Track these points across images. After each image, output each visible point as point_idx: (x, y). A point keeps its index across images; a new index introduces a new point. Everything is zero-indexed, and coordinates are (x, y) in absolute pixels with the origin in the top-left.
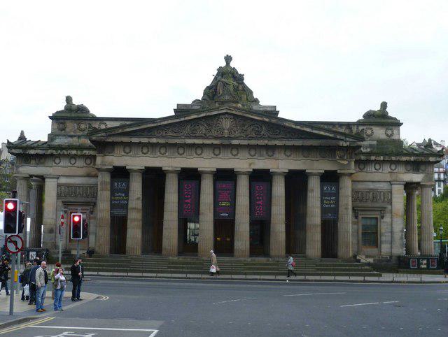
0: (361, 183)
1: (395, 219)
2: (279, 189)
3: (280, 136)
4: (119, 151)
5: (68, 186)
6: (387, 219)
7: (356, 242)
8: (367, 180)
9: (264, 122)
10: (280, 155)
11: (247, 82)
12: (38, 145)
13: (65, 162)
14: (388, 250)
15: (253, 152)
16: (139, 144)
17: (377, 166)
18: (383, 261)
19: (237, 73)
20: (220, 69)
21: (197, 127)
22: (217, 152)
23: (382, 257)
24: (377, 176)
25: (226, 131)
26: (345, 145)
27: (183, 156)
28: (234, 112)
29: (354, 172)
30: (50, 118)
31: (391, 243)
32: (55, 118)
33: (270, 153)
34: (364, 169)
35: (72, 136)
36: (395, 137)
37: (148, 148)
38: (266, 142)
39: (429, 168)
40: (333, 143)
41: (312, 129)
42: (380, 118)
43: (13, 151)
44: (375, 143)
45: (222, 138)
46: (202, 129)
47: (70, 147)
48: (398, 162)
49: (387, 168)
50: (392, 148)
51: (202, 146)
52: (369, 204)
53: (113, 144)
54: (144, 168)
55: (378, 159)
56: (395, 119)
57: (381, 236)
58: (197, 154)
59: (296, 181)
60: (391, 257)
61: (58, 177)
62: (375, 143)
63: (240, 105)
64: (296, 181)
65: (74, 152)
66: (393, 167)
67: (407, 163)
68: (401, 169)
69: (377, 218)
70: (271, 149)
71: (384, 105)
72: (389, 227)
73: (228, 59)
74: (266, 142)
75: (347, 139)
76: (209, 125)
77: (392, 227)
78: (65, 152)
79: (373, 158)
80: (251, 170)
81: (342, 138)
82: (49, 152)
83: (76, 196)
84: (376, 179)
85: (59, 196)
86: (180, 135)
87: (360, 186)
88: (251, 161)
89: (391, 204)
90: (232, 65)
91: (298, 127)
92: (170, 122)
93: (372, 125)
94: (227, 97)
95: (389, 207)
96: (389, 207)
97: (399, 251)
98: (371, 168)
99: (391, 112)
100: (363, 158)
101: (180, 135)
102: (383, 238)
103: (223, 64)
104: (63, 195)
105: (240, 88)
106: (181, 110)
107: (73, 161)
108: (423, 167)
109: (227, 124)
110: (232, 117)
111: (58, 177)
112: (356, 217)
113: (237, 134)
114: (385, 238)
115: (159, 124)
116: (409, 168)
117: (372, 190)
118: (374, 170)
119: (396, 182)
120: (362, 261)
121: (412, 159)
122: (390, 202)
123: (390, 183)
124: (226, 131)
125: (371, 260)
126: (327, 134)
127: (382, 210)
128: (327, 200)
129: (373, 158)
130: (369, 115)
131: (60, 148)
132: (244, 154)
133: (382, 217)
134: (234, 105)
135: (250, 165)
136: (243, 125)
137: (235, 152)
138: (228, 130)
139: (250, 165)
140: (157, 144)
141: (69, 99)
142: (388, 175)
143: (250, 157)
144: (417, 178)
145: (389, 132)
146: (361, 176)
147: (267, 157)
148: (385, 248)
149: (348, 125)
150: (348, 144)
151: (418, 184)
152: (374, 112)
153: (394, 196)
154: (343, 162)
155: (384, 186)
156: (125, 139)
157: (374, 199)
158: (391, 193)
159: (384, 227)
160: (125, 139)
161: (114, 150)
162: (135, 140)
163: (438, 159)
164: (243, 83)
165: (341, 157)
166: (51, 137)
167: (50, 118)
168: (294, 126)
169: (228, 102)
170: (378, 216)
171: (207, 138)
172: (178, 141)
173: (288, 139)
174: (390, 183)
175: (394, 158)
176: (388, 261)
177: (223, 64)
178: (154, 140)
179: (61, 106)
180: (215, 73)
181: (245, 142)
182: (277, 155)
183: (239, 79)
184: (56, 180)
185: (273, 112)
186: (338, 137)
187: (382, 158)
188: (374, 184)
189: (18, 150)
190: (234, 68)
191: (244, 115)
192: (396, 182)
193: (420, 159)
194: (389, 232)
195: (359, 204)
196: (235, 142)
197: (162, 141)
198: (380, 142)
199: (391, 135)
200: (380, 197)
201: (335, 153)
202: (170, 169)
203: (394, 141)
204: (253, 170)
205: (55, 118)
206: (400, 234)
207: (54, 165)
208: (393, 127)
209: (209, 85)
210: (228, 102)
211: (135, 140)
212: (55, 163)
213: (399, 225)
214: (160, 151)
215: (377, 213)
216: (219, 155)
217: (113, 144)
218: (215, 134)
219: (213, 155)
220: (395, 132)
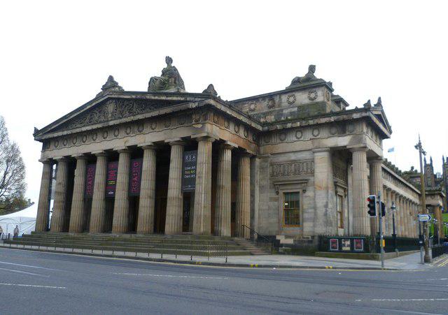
2: (148, 163)
4: (52, 146)
6: (310, 193)
9: (136, 100)
10: (147, 129)
14: (311, 229)
16: (63, 137)
17: (299, 135)
23: (304, 238)
24: (299, 145)
26: (194, 105)
28: (113, 96)
31: (314, 219)
40: (183, 107)
42: (331, 84)
48: (318, 126)
49: (308, 135)
50: (314, 112)
52: (292, 177)
55: (294, 125)
57: (302, 213)
59: (162, 151)
60: (313, 237)
62: (296, 109)
64: (162, 151)
66: (316, 132)
68: (324, 133)
70: (139, 124)
71: (312, 68)
73: (169, 60)
76: (100, 112)
77: (315, 202)
81: (192, 99)
84: (298, 149)
87: (282, 159)
89: (314, 176)
90: (173, 65)
91: (156, 98)
92: (76, 115)
93: (294, 91)
95: (312, 178)
96: (312, 178)
98: (292, 137)
99: (318, 75)
100: (279, 127)
102: (306, 215)
103: (166, 66)
108: (350, 128)
112: (277, 193)
116: (334, 130)
117: (294, 161)
118: (295, 139)
120: (281, 242)
121: (332, 119)
122: (313, 173)
125: (291, 241)
126: (179, 98)
128: (188, 170)
129: (289, 125)
130: (296, 81)
132: (122, 133)
133: (304, 191)
144: (343, 141)
145: (313, 95)
149: (270, 96)
150: (197, 104)
156: (50, 136)
157: (297, 172)
158: (313, 161)
159: (305, 202)
162: (56, 135)
168: (153, 98)
170: (301, 191)
175: (311, 122)
176: (311, 242)
177: (166, 66)
178: (65, 133)
186: (188, 99)
187: (298, 124)
188: (296, 154)
194: (311, 208)
195: (281, 178)
196: (111, 123)
197: (69, 132)
198: (301, 107)
208: (317, 89)
211: (56, 135)
215: (299, 186)
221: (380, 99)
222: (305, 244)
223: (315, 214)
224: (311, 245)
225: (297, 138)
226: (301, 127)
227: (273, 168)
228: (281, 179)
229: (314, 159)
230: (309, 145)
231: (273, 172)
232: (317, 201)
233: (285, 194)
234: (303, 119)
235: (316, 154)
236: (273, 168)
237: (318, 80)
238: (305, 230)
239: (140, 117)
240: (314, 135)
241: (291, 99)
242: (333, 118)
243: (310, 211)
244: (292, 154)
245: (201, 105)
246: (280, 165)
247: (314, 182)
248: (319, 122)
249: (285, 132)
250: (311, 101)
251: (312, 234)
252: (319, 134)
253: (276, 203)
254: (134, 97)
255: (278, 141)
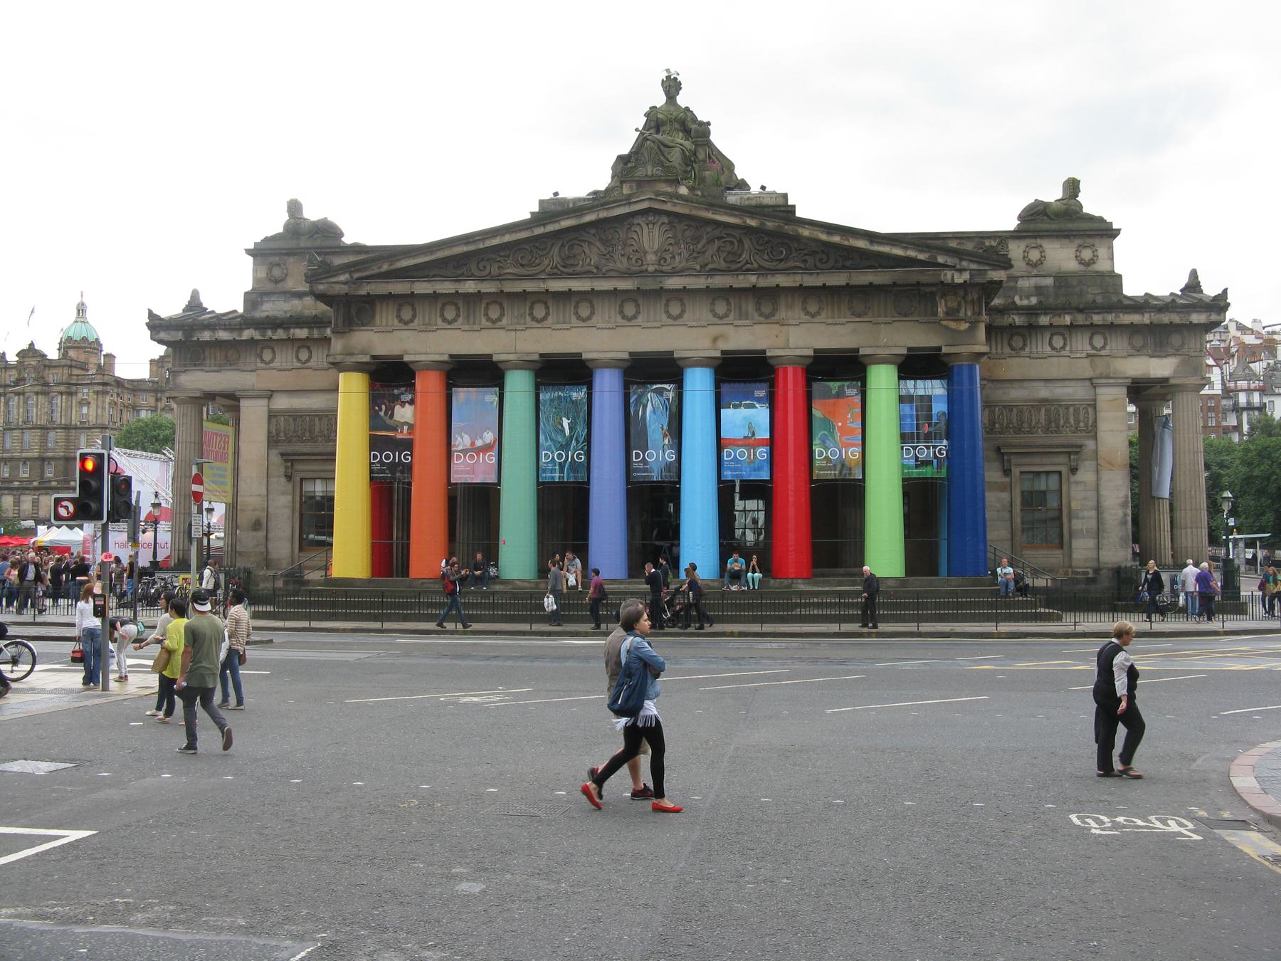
0: (1017, 385)
1: (1106, 476)
3: (791, 264)
4: (386, 316)
5: (295, 415)
6: (1086, 474)
7: (1009, 536)
8: (1033, 375)
9: (748, 230)
10: (791, 312)
11: (718, 139)
12: (221, 322)
13: (284, 358)
15: (721, 308)
16: (435, 296)
17: (1058, 341)
18: (1077, 582)
19: (694, 119)
20: (652, 114)
21: (577, 250)
22: (630, 309)
23: (1074, 572)
24: (1056, 367)
25: (651, 258)
26: (959, 279)
27: (545, 324)
28: (668, 207)
29: (984, 349)
30: (249, 252)
31: (1098, 534)
32: (260, 253)
33: (766, 309)
34: (1023, 348)
35: (300, 295)
36: (1101, 266)
37: (458, 309)
38: (753, 279)
39: (1192, 343)
40: (926, 276)
41: (872, 242)
43: (162, 335)
44: (1049, 281)
45: (642, 274)
46: (592, 254)
47: (298, 322)
49: (1081, 343)
50: (1093, 293)
51: (589, 296)
52: (1040, 438)
53: (370, 302)
54: (446, 358)
56: (1101, 220)
57: (1070, 521)
58: (579, 318)
60: (1097, 571)
61: (270, 395)
62: (1049, 281)
63: (683, 190)
65: (302, 333)
66: (1098, 341)
67: (1133, 329)
68: (1118, 344)
69: (1060, 473)
70: (766, 298)
71: (1072, 187)
72: (1092, 494)
73: (672, 86)
74: (753, 279)
75: (965, 264)
76: (605, 242)
78: (281, 334)
79: (1044, 320)
80: (718, 354)
81: (950, 261)
82: (247, 334)
83: (313, 439)
84: (1054, 375)
85: (272, 441)
86: (533, 270)
87: (1015, 394)
88: (715, 330)
89: (1095, 438)
90: (682, 100)
91: (836, 239)
92: (508, 238)
93: (1041, 237)
94: (650, 170)
95: (1090, 444)
97: (1117, 553)
98: (1041, 346)
99: (1090, 204)
100: (1018, 320)
101: (533, 270)
102: (1077, 524)
103: (660, 100)
104: (282, 437)
105: (701, 155)
106: (552, 210)
107: (304, 355)
108: (1176, 340)
109: (651, 238)
110: (665, 219)
111: (270, 395)
112: (1007, 472)
113: (678, 263)
114: (1083, 522)
115: (481, 246)
116: (1138, 341)
117: (1044, 401)
119: (1107, 378)
122: (1093, 432)
123: (1092, 382)
124: (651, 258)
126: (912, 253)
127: (1073, 453)
129: (1044, 320)
131: (274, 323)
132: (698, 312)
133: (1074, 470)
134: (669, 189)
135: (715, 340)
136: (696, 240)
137: (675, 309)
138: (656, 253)
139: (715, 340)
140: (479, 295)
141: (294, 208)
142: (1087, 361)
143: (716, 320)
144: (1160, 367)
145: (1087, 254)
146: (1014, 367)
147: (756, 316)
148: (1082, 550)
150: (966, 276)
151: (1164, 381)
152: (1046, 205)
153: (1101, 415)
154: (953, 325)
155: (1077, 392)
156: (399, 287)
157: (1052, 425)
158: (1094, 406)
159: (1078, 494)
160: (399, 287)
161: (373, 317)
162: (422, 288)
163: (1214, 317)
164: (709, 144)
165: (952, 314)
166: (252, 299)
167: (249, 252)
168: (824, 237)
169: (652, 180)
170: (1064, 469)
171: (605, 276)
172: (530, 286)
173: (807, 270)
174: (1092, 382)
175: (1097, 319)
176: (1092, 581)
177: (660, 100)
178: (470, 287)
179: (275, 224)
180: (641, 122)
181: (701, 283)
182: (782, 314)
183: (696, 131)
184: (265, 402)
185: (781, 210)
186: (941, 259)
187: (1067, 320)
189: (173, 333)
190: (687, 109)
191: (695, 213)
192: (1107, 378)
193: (1165, 318)
195: (1011, 438)
196: (674, 283)
198: (1062, 280)
199: (1092, 261)
200: (1067, 421)
201: (935, 306)
202: (511, 357)
203: (1101, 275)
204: (723, 352)
205: (260, 253)
206: (1120, 512)
207: (261, 365)
208: (1097, 241)
209: (626, 150)
210: (652, 180)
211: (422, 288)
212: (262, 361)
213: (1116, 490)
214: (486, 315)
215: (1063, 459)
216: (635, 317)
217: (370, 302)
218: (622, 264)
219: (619, 318)
220: (1102, 252)
221: (1194, 274)
222: (1078, 587)
223: (1099, 520)
224: (1092, 587)
225: (1053, 348)
226: (1072, 327)
227: (992, 413)
228: (1013, 441)
229: (1095, 400)
230: (1084, 368)
231: (993, 423)
232: (1103, 493)
233: (1021, 472)
234: (1080, 311)
235: (1100, 391)
236: (992, 413)
237: (1091, 218)
238: (1074, 556)
239: (783, 281)
240: (1094, 348)
241: (1034, 255)
242: (1147, 315)
243: (1086, 514)
244: (1042, 384)
245: (978, 280)
246: (1010, 408)
247: (1096, 451)
248: (1117, 322)
249: (1032, 329)
250: (1082, 268)
251: (1095, 564)
252: (1105, 344)
253: (1005, 496)
254: (753, 223)
255: (1007, 350)
